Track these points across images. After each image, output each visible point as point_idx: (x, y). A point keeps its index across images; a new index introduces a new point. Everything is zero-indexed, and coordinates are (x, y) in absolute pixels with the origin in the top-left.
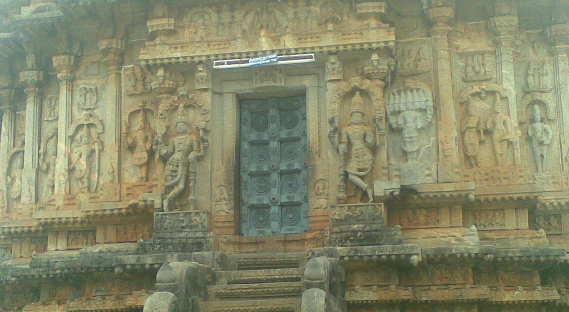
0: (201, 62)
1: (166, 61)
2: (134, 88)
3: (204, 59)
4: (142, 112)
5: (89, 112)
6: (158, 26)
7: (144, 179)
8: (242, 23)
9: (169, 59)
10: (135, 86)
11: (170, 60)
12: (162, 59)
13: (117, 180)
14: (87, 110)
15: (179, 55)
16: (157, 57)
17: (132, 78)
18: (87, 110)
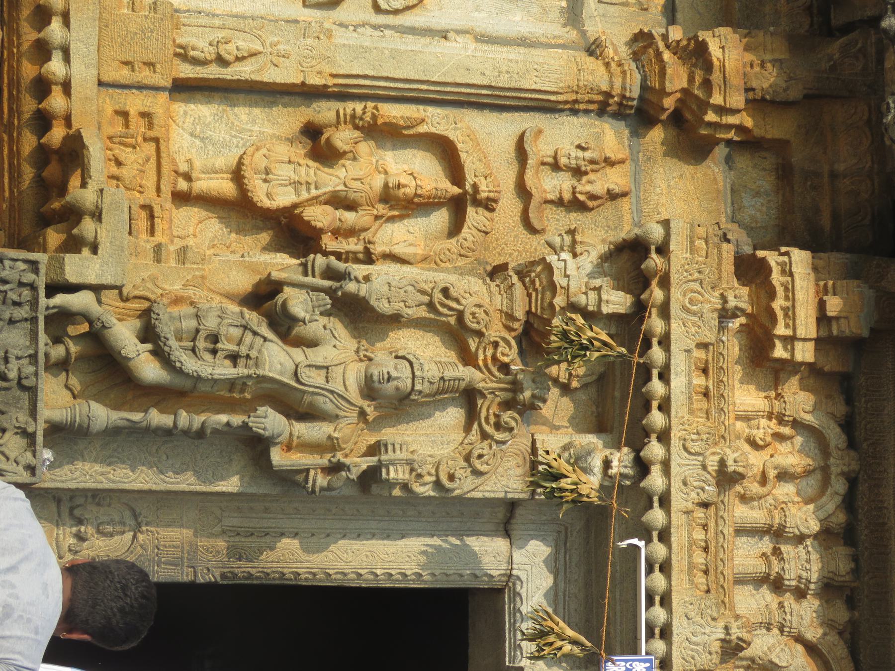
0: (642, 467)
1: (656, 324)
2: (550, 160)
3: (656, 480)
4: (456, 190)
6: (790, 291)
7: (183, 185)
8: (775, 631)
9: (665, 342)
10: (556, 166)
11: (660, 343)
12: (665, 311)
13: (187, 71)
15: (678, 382)
16: (676, 295)
17: (588, 155)
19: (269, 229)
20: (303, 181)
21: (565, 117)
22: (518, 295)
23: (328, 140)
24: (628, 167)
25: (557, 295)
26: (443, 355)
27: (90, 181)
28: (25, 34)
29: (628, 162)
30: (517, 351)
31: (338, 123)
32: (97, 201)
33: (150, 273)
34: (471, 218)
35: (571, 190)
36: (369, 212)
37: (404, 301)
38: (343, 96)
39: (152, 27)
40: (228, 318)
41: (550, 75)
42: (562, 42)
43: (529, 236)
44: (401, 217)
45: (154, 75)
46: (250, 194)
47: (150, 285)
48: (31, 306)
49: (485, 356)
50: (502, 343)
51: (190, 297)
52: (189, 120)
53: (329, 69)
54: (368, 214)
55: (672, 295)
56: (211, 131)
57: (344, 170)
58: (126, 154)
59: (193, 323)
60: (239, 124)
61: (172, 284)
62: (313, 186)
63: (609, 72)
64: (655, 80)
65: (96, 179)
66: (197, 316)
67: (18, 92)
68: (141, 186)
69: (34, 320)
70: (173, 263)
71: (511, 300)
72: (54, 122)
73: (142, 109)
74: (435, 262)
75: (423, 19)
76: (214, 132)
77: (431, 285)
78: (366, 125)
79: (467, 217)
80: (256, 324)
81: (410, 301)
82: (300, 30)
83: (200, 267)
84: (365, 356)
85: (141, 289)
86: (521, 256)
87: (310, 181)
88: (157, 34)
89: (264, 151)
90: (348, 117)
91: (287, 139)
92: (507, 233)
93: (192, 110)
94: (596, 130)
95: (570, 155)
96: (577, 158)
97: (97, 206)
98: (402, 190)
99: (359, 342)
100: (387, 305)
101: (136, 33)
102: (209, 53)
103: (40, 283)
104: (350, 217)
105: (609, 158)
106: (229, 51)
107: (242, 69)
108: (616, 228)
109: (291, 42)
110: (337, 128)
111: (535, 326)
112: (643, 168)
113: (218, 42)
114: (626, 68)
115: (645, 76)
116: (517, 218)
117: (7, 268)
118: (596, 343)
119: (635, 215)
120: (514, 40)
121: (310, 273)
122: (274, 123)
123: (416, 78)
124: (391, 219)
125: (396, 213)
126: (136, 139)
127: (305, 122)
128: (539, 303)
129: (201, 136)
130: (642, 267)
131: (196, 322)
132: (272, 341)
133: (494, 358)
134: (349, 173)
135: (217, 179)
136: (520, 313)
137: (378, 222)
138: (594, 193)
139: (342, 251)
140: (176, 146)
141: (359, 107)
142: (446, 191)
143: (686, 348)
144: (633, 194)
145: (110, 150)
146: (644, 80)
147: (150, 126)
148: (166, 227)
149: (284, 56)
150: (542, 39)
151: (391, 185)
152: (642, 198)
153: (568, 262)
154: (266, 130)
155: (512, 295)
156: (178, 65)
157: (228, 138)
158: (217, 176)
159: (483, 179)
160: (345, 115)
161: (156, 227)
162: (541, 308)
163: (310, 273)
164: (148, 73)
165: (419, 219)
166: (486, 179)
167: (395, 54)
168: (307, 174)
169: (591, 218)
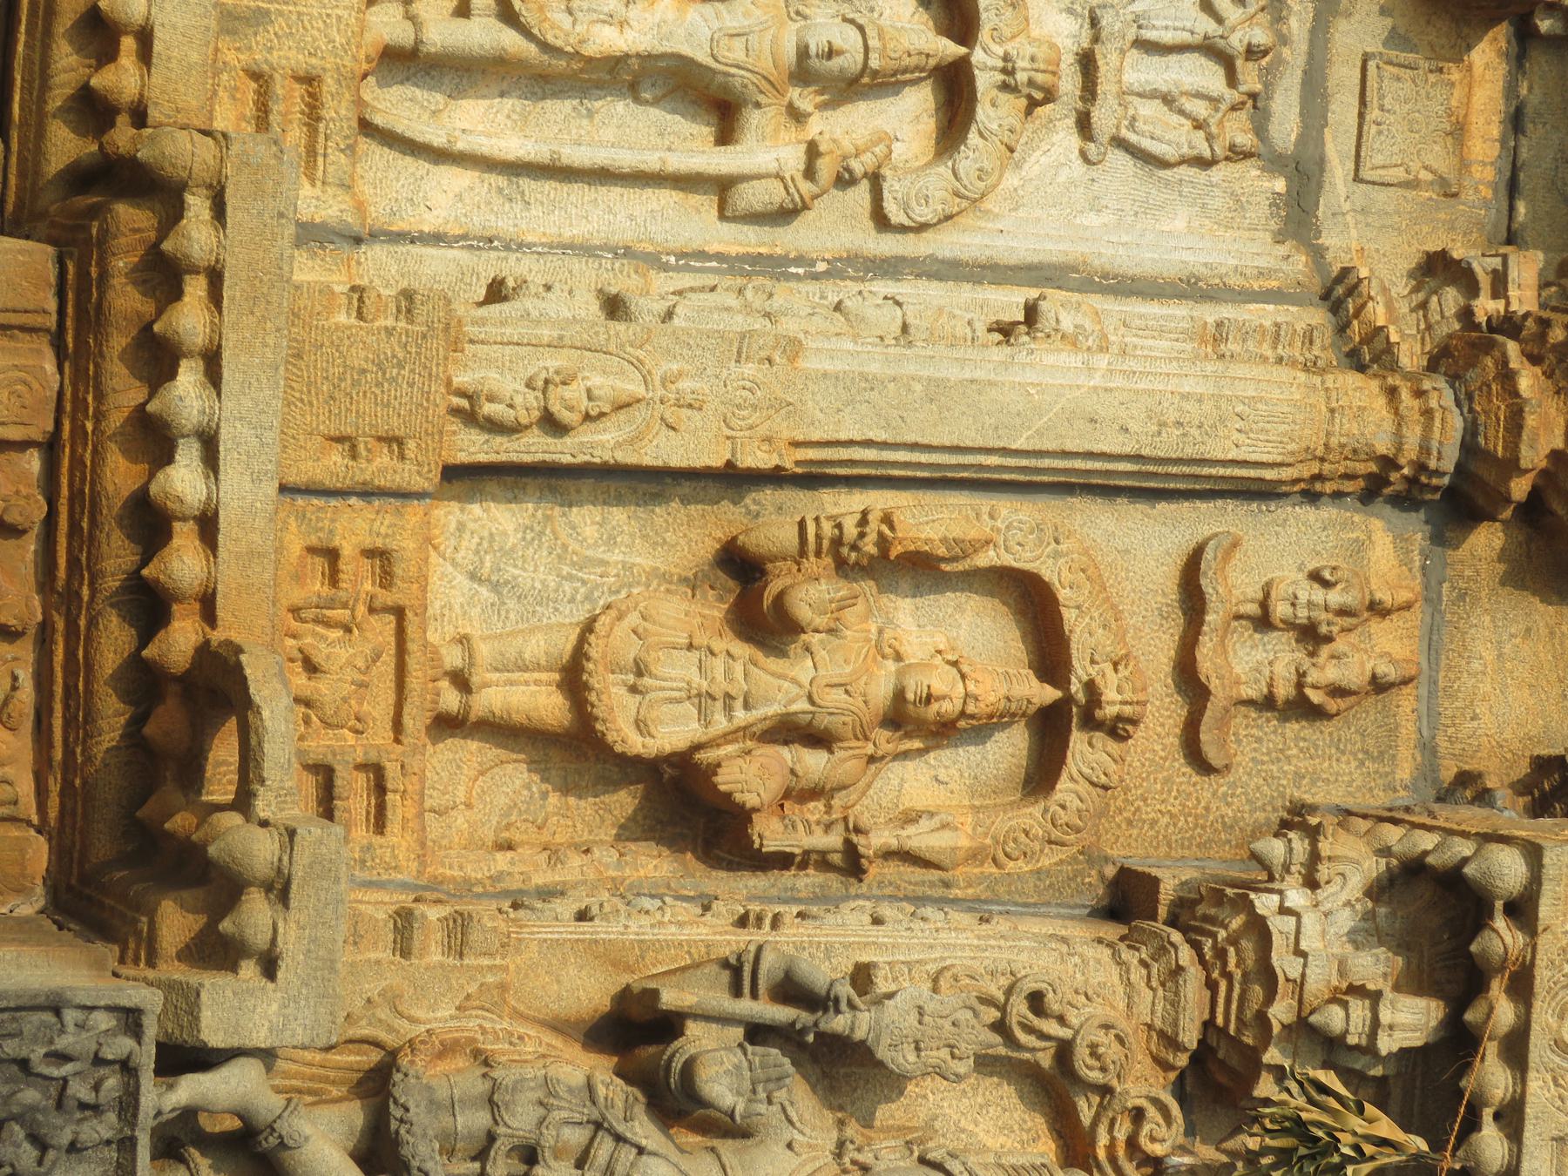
2: (1253, 609)
4: (1050, 694)
5: (1069, 84)
7: (451, 700)
9: (1512, 1117)
10: (1263, 622)
11: (1497, 1116)
12: (1516, 1050)
13: (474, 447)
14: (1087, 63)
16: (1543, 1016)
17: (1335, 597)
18: (1087, 63)
19: (631, 784)
20: (719, 694)
21: (1290, 509)
22: (1190, 995)
23: (780, 598)
24: (1416, 617)
25: (1278, 997)
26: (1016, 1127)
27: (261, 791)
28: (114, 390)
29: (1417, 605)
30: (1182, 1130)
31: (803, 552)
32: (280, 860)
33: (384, 983)
34: (1078, 757)
35: (1294, 678)
36: (857, 752)
37: (951, 1047)
38: (812, 479)
39: (401, 355)
40: (560, 1108)
41: (1269, 426)
42: (1274, 284)
43: (1195, 778)
44: (921, 752)
45: (400, 466)
46: (599, 726)
47: (383, 1013)
48: (121, 1109)
49: (1113, 1139)
50: (1152, 1112)
51: (473, 1040)
52: (469, 542)
53: (787, 432)
54: (854, 757)
55: (1534, 1016)
56: (515, 566)
57: (809, 663)
58: (329, 646)
59: (482, 1119)
60: (577, 547)
61: (433, 1008)
62: (739, 703)
63: (1397, 413)
64: (1496, 437)
65: (276, 785)
66: (491, 1101)
67: (93, 522)
68: (358, 719)
69: (127, 1145)
70: (435, 956)
71: (1175, 1004)
72: (175, 607)
73: (368, 543)
74: (994, 860)
75: (978, 240)
76: (525, 570)
77: (1004, 982)
78: (865, 562)
79: (1069, 754)
80: (621, 1116)
81: (963, 1045)
82: (731, 344)
83: (498, 961)
84: (854, 1162)
85: (364, 1023)
86: (1175, 825)
87: (733, 694)
88: (412, 371)
89: (633, 619)
90: (826, 544)
91: (684, 580)
92: (1149, 774)
93: (475, 521)
94: (1354, 535)
95: (1296, 597)
96: (1310, 604)
97: (279, 870)
98: (935, 707)
99: (841, 1123)
100: (912, 1058)
101: (364, 371)
102: (526, 405)
103: (144, 1060)
104: (813, 762)
105: (1380, 602)
106: (568, 401)
107: (597, 438)
108: (1381, 753)
109: (709, 372)
110: (798, 564)
111: (1221, 1055)
112: (1448, 617)
113: (547, 382)
114: (1433, 403)
115: (1475, 423)
116: (1174, 741)
117: (71, 1028)
118: (1369, 1149)
119: (1425, 722)
120: (1172, 284)
121: (747, 989)
122: (656, 543)
123: (980, 443)
124: (905, 755)
125: (917, 744)
126: (353, 610)
127: (724, 539)
128: (1234, 1006)
129: (494, 578)
130: (1473, 948)
131: (489, 1116)
132: (655, 1154)
133: (1132, 1144)
134: (822, 672)
135: (527, 683)
136: (1190, 1036)
137: (873, 767)
138: (1344, 684)
139: (797, 851)
140: (437, 604)
141: (846, 505)
142: (1029, 702)
143: (1555, 1133)
144: (1423, 679)
145: (294, 637)
146: (1471, 431)
147: (386, 578)
148: (411, 812)
149: (690, 406)
150: (1234, 281)
151: (910, 696)
152: (1441, 684)
153: (1305, 920)
154: (638, 560)
155: (1177, 994)
156: (454, 433)
157: (552, 581)
158: (526, 675)
159: (1108, 667)
160: (818, 537)
161: (389, 814)
162: (1238, 1018)
163: (747, 989)
164: (386, 459)
165: (960, 750)
166: (1116, 670)
167: (936, 390)
168: (728, 672)
169: (1331, 734)
